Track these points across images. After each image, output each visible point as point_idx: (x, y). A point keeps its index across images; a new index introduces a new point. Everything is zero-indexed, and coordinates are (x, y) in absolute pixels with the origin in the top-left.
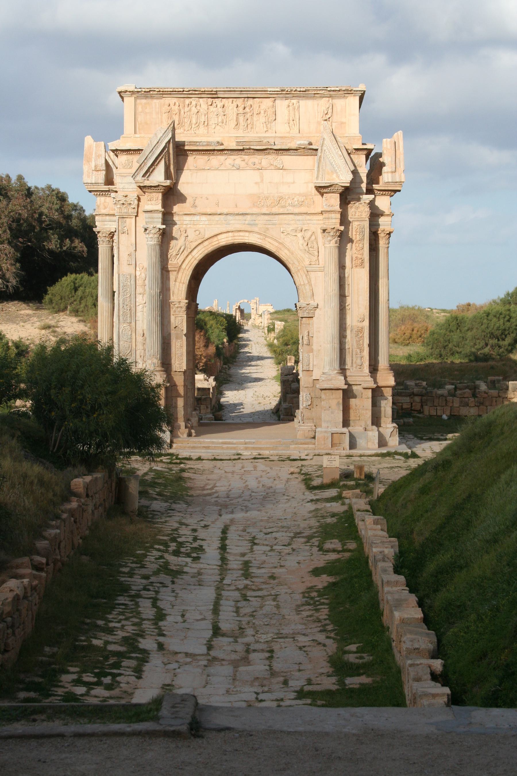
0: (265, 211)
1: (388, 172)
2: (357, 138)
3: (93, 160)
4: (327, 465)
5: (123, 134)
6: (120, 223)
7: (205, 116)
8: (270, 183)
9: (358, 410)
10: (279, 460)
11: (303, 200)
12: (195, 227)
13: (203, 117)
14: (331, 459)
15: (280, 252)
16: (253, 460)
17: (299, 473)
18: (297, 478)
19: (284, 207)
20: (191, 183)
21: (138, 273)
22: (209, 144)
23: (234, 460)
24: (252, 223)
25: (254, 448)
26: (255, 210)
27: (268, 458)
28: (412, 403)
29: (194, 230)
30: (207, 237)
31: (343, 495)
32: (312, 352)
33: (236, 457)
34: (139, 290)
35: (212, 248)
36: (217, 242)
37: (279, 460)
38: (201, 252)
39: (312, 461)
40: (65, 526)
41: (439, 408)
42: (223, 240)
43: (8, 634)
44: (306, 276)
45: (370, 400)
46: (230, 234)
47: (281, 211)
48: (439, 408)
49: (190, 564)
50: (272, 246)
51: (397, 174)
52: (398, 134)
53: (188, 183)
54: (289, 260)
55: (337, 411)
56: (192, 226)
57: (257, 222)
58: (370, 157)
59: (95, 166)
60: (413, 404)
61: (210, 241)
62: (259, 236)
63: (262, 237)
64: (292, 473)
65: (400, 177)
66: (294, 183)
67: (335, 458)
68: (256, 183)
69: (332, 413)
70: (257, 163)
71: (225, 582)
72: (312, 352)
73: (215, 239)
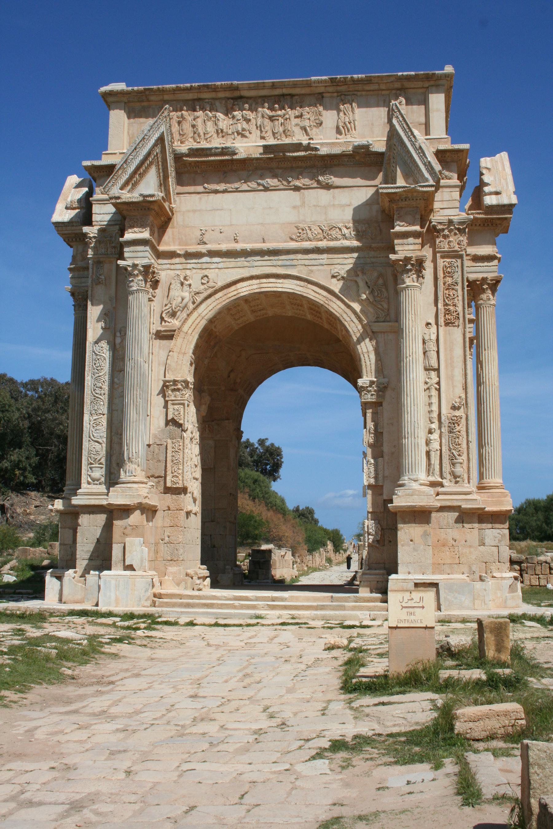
0: (307, 245)
1: (491, 194)
2: (443, 140)
4: (399, 621)
5: (106, 149)
6: (95, 269)
9: (456, 548)
10: (324, 627)
11: (364, 228)
12: (204, 271)
14: (410, 604)
15: (331, 304)
16: (280, 627)
17: (346, 648)
18: (336, 658)
19: (336, 239)
20: (199, 211)
22: (224, 151)
23: (249, 625)
24: (288, 263)
25: (285, 607)
26: (293, 245)
27: (305, 623)
29: (201, 275)
30: (220, 284)
31: (459, 727)
32: (382, 457)
33: (254, 621)
35: (228, 301)
36: (235, 293)
37: (324, 627)
38: (211, 307)
39: (381, 628)
41: (541, 576)
42: (244, 289)
46: (255, 281)
47: (332, 244)
50: (317, 296)
51: (504, 195)
52: (501, 157)
53: (194, 211)
54: (345, 316)
55: (422, 547)
56: (199, 271)
57: (295, 262)
61: (225, 291)
62: (298, 282)
63: (302, 283)
64: (331, 648)
65: (510, 198)
67: (421, 599)
68: (294, 207)
69: (415, 550)
72: (382, 457)
73: (233, 288)
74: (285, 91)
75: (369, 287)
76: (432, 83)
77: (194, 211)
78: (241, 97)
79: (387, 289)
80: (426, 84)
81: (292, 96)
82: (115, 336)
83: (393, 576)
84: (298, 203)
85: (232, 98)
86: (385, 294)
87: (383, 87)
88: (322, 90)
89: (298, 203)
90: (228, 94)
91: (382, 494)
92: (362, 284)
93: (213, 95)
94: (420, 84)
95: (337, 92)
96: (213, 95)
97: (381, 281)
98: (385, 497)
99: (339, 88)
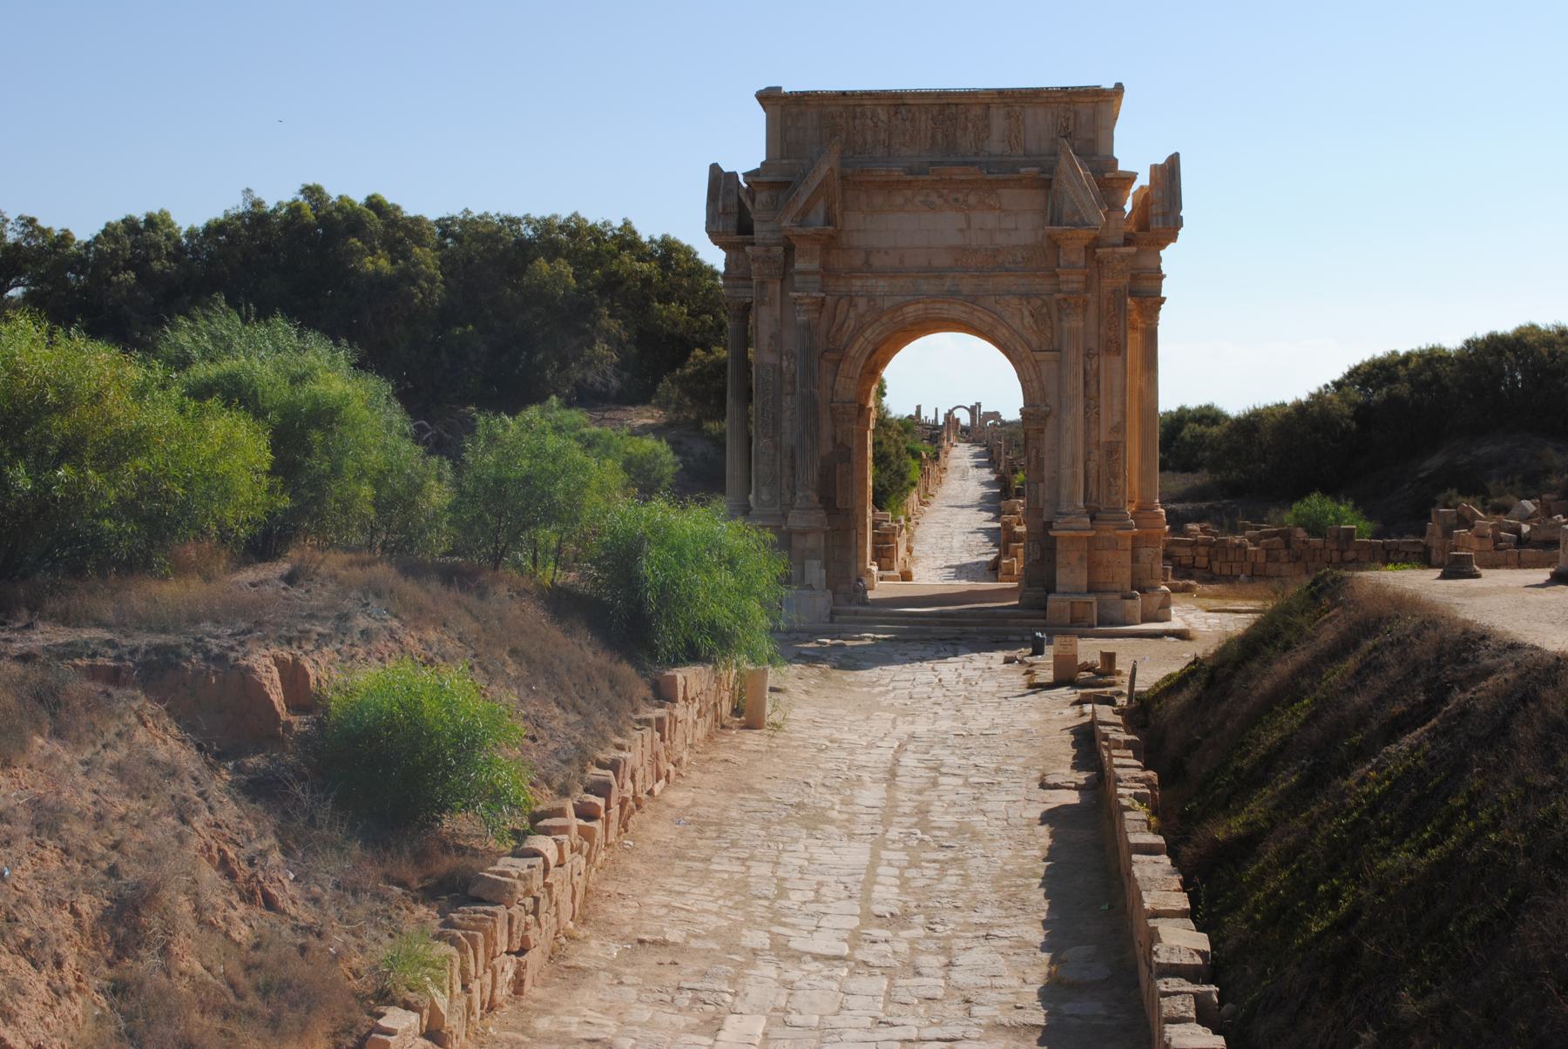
3: (720, 197)
7: (885, 132)
8: (981, 229)
13: (882, 133)
21: (785, 364)
28: (1194, 558)
32: (1043, 481)
34: (788, 388)
40: (643, 746)
41: (1234, 565)
43: (527, 924)
44: (1034, 368)
45: (1129, 553)
48: (1234, 565)
49: (837, 807)
53: (859, 231)
58: (1132, 191)
59: (724, 207)
60: (1197, 558)
66: (1016, 229)
68: (961, 230)
70: (961, 200)
71: (888, 836)
74: (950, 101)
75: (1033, 316)
76: (1101, 98)
77: (859, 231)
78: (904, 104)
79: (1050, 318)
80: (1096, 99)
81: (957, 105)
82: (781, 359)
83: (1051, 597)
84: (964, 226)
85: (895, 105)
86: (1049, 322)
87: (1052, 100)
88: (989, 101)
89: (964, 226)
90: (890, 102)
91: (1041, 516)
92: (1026, 313)
93: (876, 102)
94: (1090, 99)
95: (1005, 103)
96: (876, 102)
97: (1045, 310)
98: (1045, 520)
99: (1007, 100)
